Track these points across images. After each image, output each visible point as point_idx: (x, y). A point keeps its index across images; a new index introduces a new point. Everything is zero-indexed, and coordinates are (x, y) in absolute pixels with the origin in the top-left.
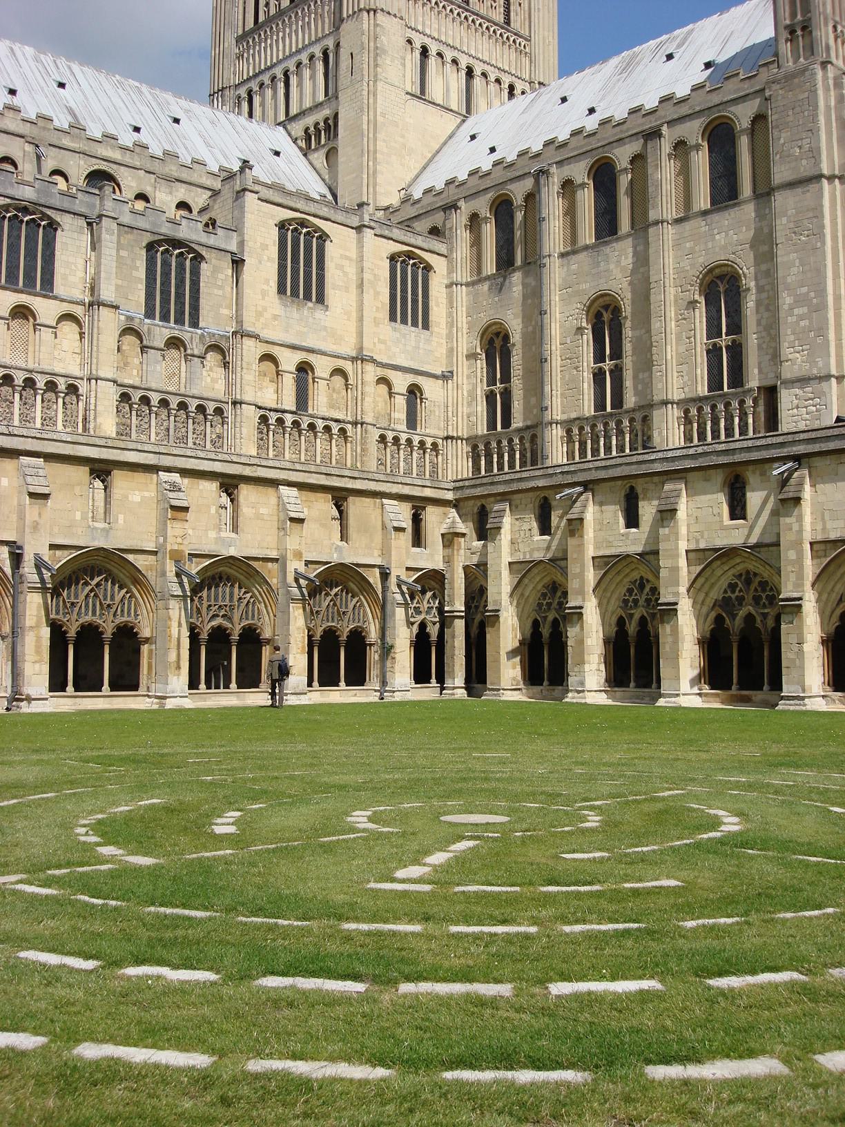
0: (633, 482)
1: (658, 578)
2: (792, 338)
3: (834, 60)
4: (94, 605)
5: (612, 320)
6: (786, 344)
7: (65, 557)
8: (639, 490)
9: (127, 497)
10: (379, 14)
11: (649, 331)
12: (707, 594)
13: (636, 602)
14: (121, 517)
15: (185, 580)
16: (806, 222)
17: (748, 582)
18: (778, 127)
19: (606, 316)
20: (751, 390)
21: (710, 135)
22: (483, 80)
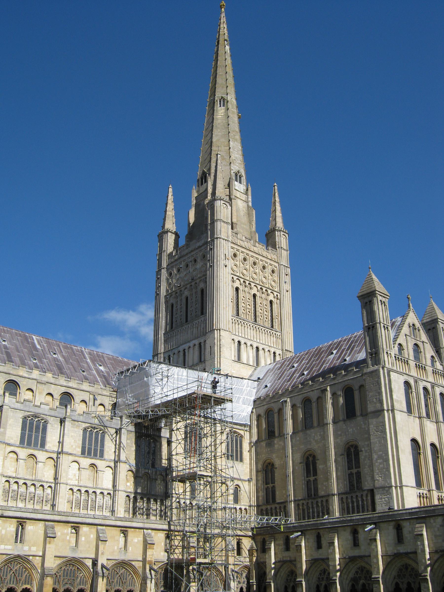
0: (319, 531)
1: (329, 569)
2: (378, 471)
3: (387, 365)
4: (120, 582)
5: (312, 461)
6: (375, 474)
7: (110, 564)
8: (321, 534)
9: (132, 540)
10: (221, 331)
11: (326, 466)
12: (348, 575)
13: (323, 578)
14: (130, 548)
15: (152, 572)
16: (380, 427)
17: (362, 570)
18: (368, 391)
19: (311, 459)
20: (364, 490)
21: (345, 391)
22: (263, 351)
